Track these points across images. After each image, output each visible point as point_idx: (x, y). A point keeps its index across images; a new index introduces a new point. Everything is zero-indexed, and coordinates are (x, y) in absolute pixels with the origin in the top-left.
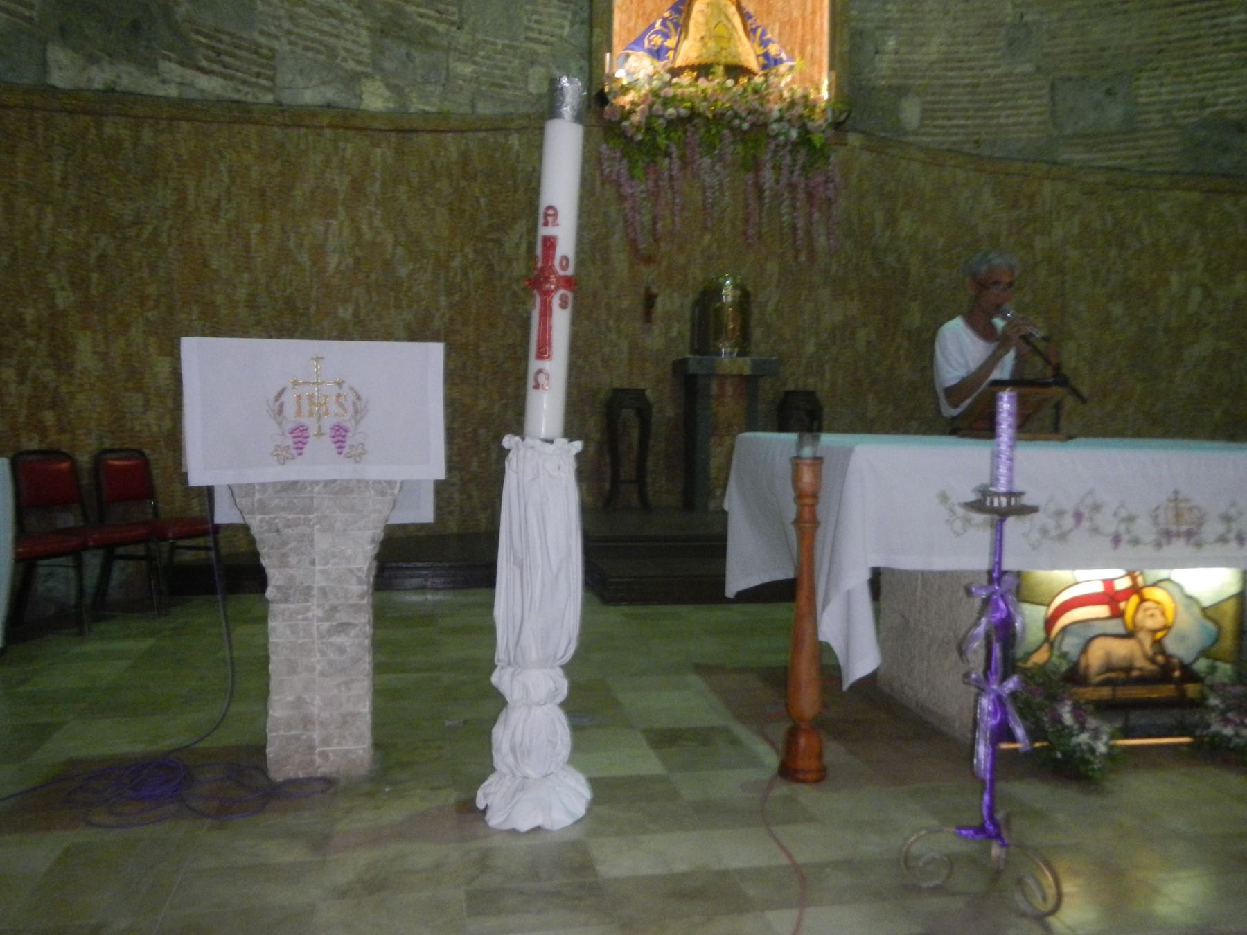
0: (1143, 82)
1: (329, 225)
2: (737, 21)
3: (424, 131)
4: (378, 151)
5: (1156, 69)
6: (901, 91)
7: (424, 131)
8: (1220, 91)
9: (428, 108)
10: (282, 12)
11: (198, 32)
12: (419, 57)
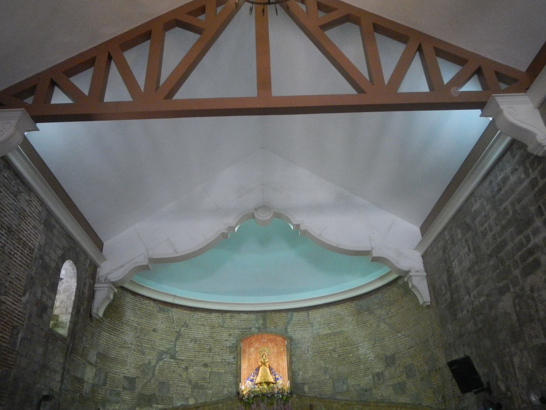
0: (349, 380)
2: (268, 371)
3: (201, 407)
6: (304, 384)
7: (201, 407)
8: (362, 382)
9: (202, 401)
11: (160, 397)
12: (200, 391)
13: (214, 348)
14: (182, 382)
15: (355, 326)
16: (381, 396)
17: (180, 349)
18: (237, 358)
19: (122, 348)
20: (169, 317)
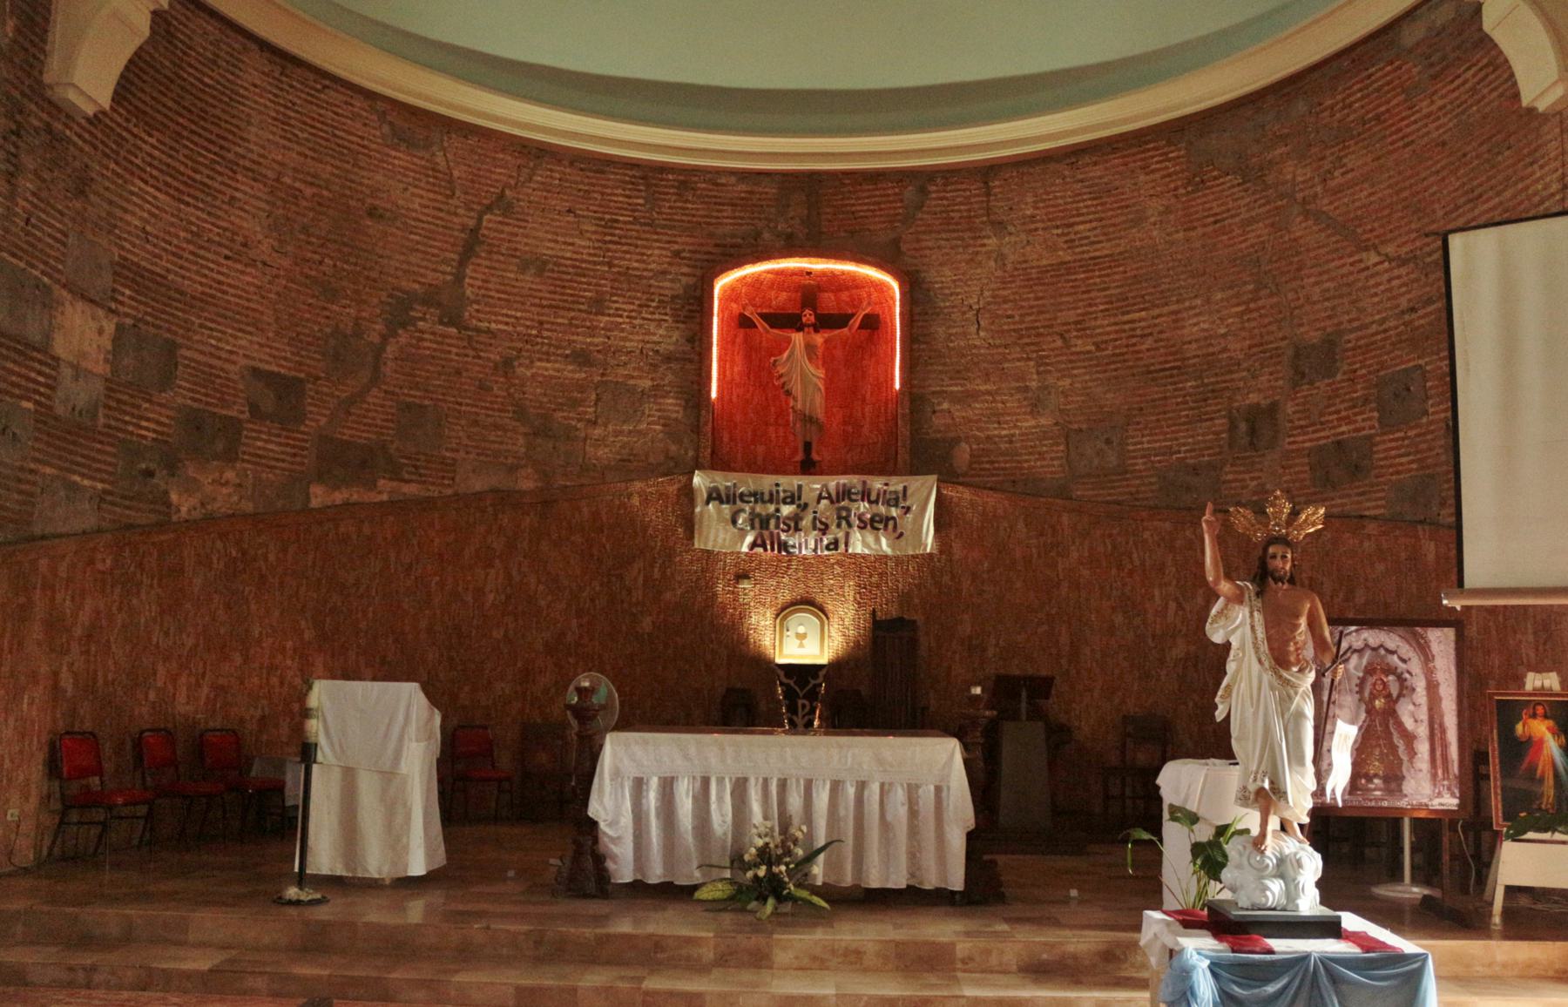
1: (487, 574)
4: (528, 520)
5: (1138, 423)
10: (461, 434)
11: (402, 457)
13: (615, 298)
14: (490, 412)
15: (1177, 232)
16: (1255, 493)
17: (483, 292)
18: (700, 340)
19: (236, 261)
20: (433, 169)
